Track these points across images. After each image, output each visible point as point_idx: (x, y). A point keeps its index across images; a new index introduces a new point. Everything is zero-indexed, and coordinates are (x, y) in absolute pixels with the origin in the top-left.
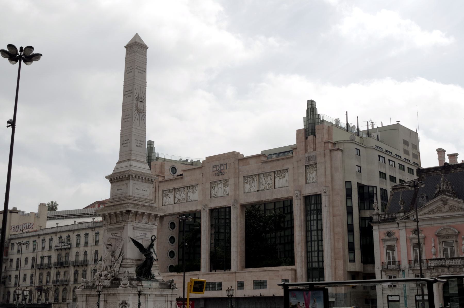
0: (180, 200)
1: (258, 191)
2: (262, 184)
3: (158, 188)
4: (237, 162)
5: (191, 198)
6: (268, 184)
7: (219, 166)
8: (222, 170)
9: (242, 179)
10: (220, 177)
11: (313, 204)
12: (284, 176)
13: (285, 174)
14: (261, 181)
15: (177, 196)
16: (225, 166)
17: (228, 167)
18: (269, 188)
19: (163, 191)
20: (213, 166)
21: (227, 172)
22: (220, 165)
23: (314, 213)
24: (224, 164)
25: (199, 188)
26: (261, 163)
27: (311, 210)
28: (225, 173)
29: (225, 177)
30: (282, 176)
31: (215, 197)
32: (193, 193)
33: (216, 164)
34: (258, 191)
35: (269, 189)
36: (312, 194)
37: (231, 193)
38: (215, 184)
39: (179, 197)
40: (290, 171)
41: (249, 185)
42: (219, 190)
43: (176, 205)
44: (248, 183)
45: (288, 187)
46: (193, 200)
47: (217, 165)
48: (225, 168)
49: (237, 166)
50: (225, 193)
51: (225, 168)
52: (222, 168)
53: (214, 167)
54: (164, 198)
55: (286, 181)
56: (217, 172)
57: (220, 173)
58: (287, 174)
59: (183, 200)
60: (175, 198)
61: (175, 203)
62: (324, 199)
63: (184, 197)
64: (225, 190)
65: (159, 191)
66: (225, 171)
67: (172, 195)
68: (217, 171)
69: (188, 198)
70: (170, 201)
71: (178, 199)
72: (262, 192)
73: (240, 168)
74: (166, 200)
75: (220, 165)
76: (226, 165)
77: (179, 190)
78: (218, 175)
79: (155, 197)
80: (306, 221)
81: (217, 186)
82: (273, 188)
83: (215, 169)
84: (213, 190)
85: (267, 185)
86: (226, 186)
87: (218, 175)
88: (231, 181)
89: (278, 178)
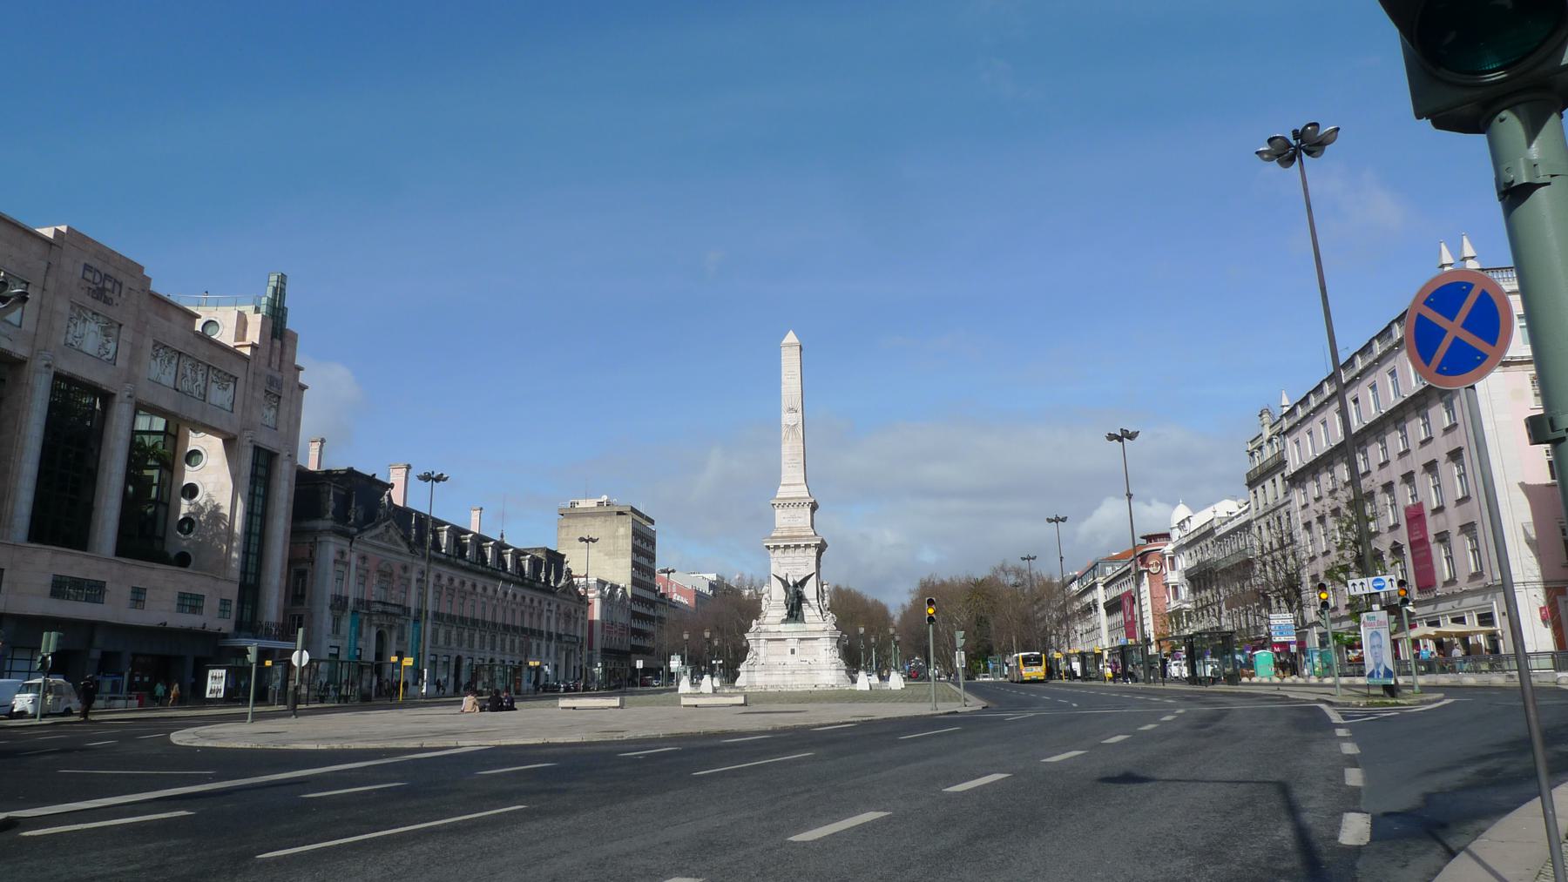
7: (101, 275)
8: (108, 290)
10: (99, 306)
17: (123, 295)
22: (105, 275)
24: (116, 281)
28: (115, 302)
29: (113, 312)
42: (90, 336)
48: (117, 292)
51: (117, 292)
53: (87, 267)
56: (93, 287)
68: (94, 283)
75: (105, 275)
78: (95, 296)
83: (89, 275)
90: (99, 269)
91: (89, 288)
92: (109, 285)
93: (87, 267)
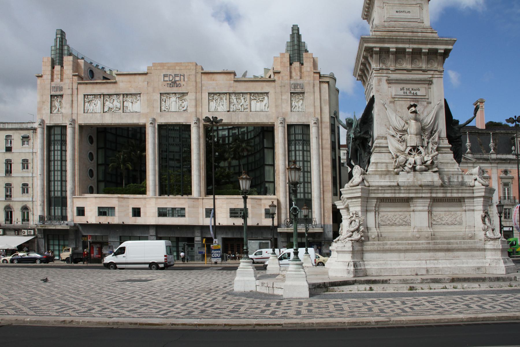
0: (112, 108)
1: (228, 111)
2: (234, 105)
3: (76, 90)
4: (199, 75)
5: (128, 108)
6: (241, 106)
8: (178, 81)
9: (205, 96)
10: (175, 90)
11: (299, 134)
12: (262, 100)
13: (264, 98)
14: (232, 101)
15: (107, 104)
16: (182, 77)
17: (186, 80)
18: (243, 110)
19: (84, 95)
20: (164, 75)
21: (185, 85)
22: (175, 75)
23: (299, 143)
24: (181, 75)
25: (143, 97)
26: (233, 82)
27: (295, 140)
28: (182, 85)
30: (260, 99)
31: (167, 111)
32: (132, 103)
33: (168, 73)
34: (228, 111)
35: (243, 111)
36: (294, 123)
37: (191, 109)
38: (167, 97)
39: (111, 105)
40: (272, 95)
41: (215, 103)
42: (173, 103)
43: (106, 114)
44: (214, 101)
45: (268, 113)
46: (131, 111)
47: (170, 75)
48: (182, 79)
49: (199, 80)
50: (181, 108)
51: (182, 79)
52: (177, 79)
53: (165, 76)
54: (86, 104)
55: (265, 105)
56: (170, 82)
57: (174, 83)
58: (266, 98)
59: (117, 109)
60: (104, 105)
61: (104, 112)
62: (313, 130)
63: (118, 106)
64: (181, 105)
65: (77, 94)
66: (182, 83)
67: (99, 101)
68: (170, 81)
69: (125, 108)
70: (95, 108)
71: (109, 108)
72: (234, 113)
73: (202, 82)
74: (90, 107)
75: (175, 75)
76: (184, 76)
77: (109, 97)
78: (171, 86)
79: (72, 101)
80: (289, 151)
81: (170, 99)
82: (248, 110)
84: (163, 102)
85: (240, 107)
86: (183, 101)
87: (171, 86)
88: (191, 97)
89: (255, 101)
90: (170, 74)
91: (168, 84)
92: (177, 79)
93: (165, 76)
